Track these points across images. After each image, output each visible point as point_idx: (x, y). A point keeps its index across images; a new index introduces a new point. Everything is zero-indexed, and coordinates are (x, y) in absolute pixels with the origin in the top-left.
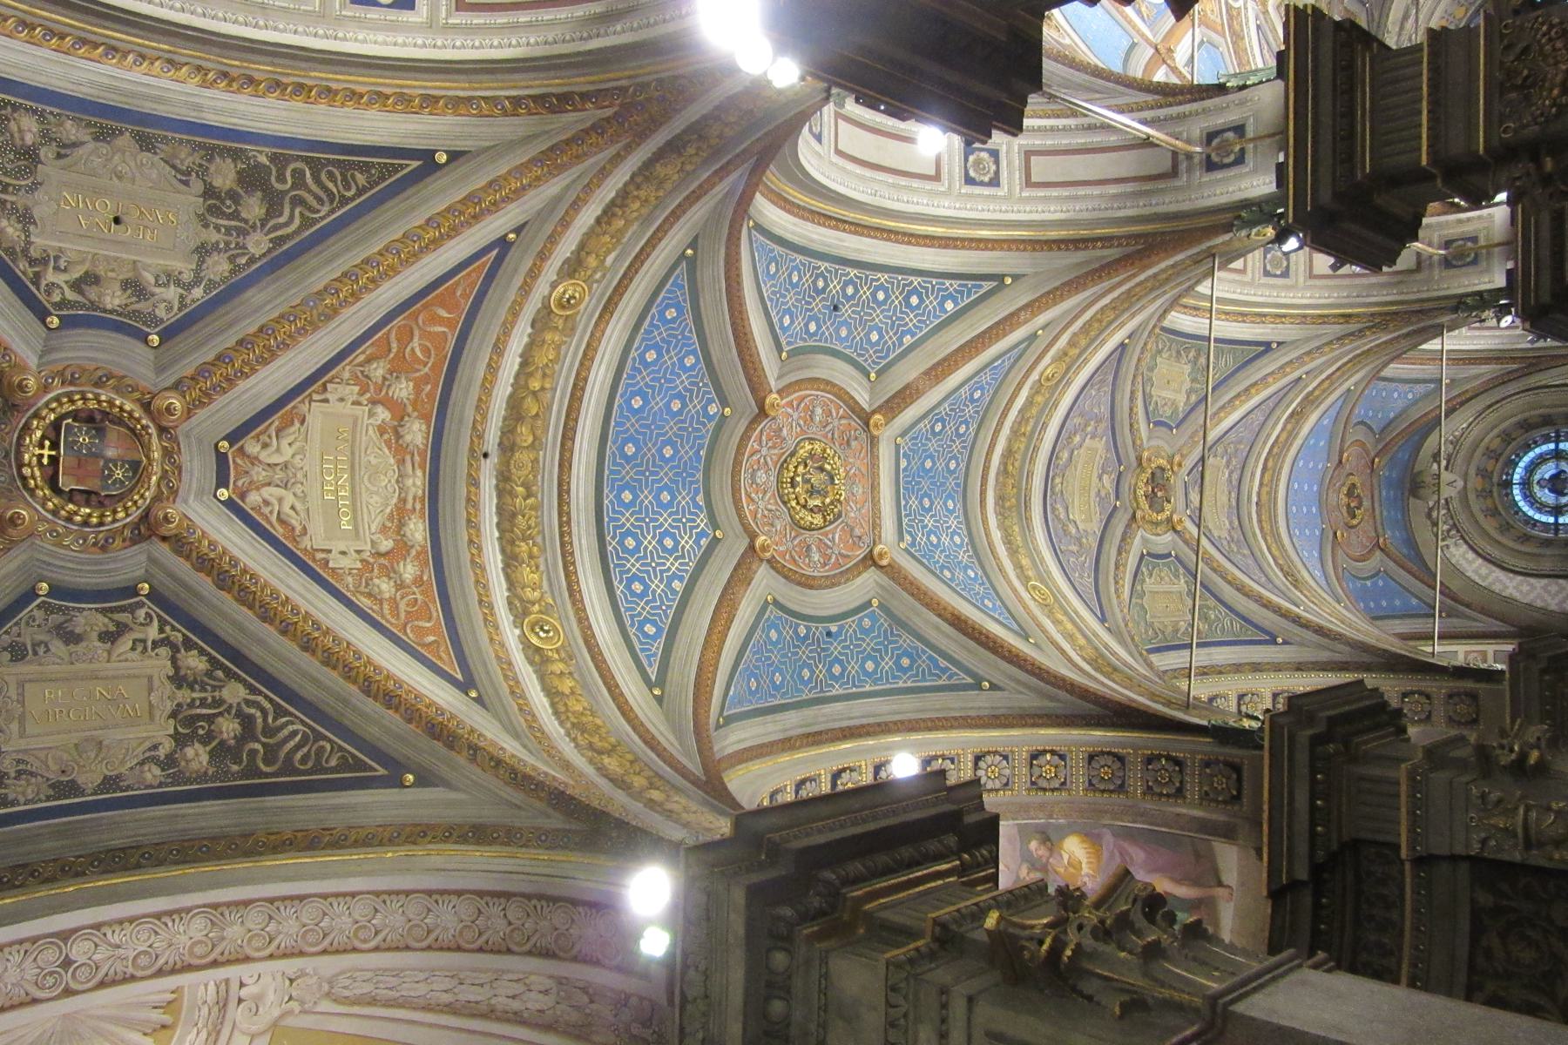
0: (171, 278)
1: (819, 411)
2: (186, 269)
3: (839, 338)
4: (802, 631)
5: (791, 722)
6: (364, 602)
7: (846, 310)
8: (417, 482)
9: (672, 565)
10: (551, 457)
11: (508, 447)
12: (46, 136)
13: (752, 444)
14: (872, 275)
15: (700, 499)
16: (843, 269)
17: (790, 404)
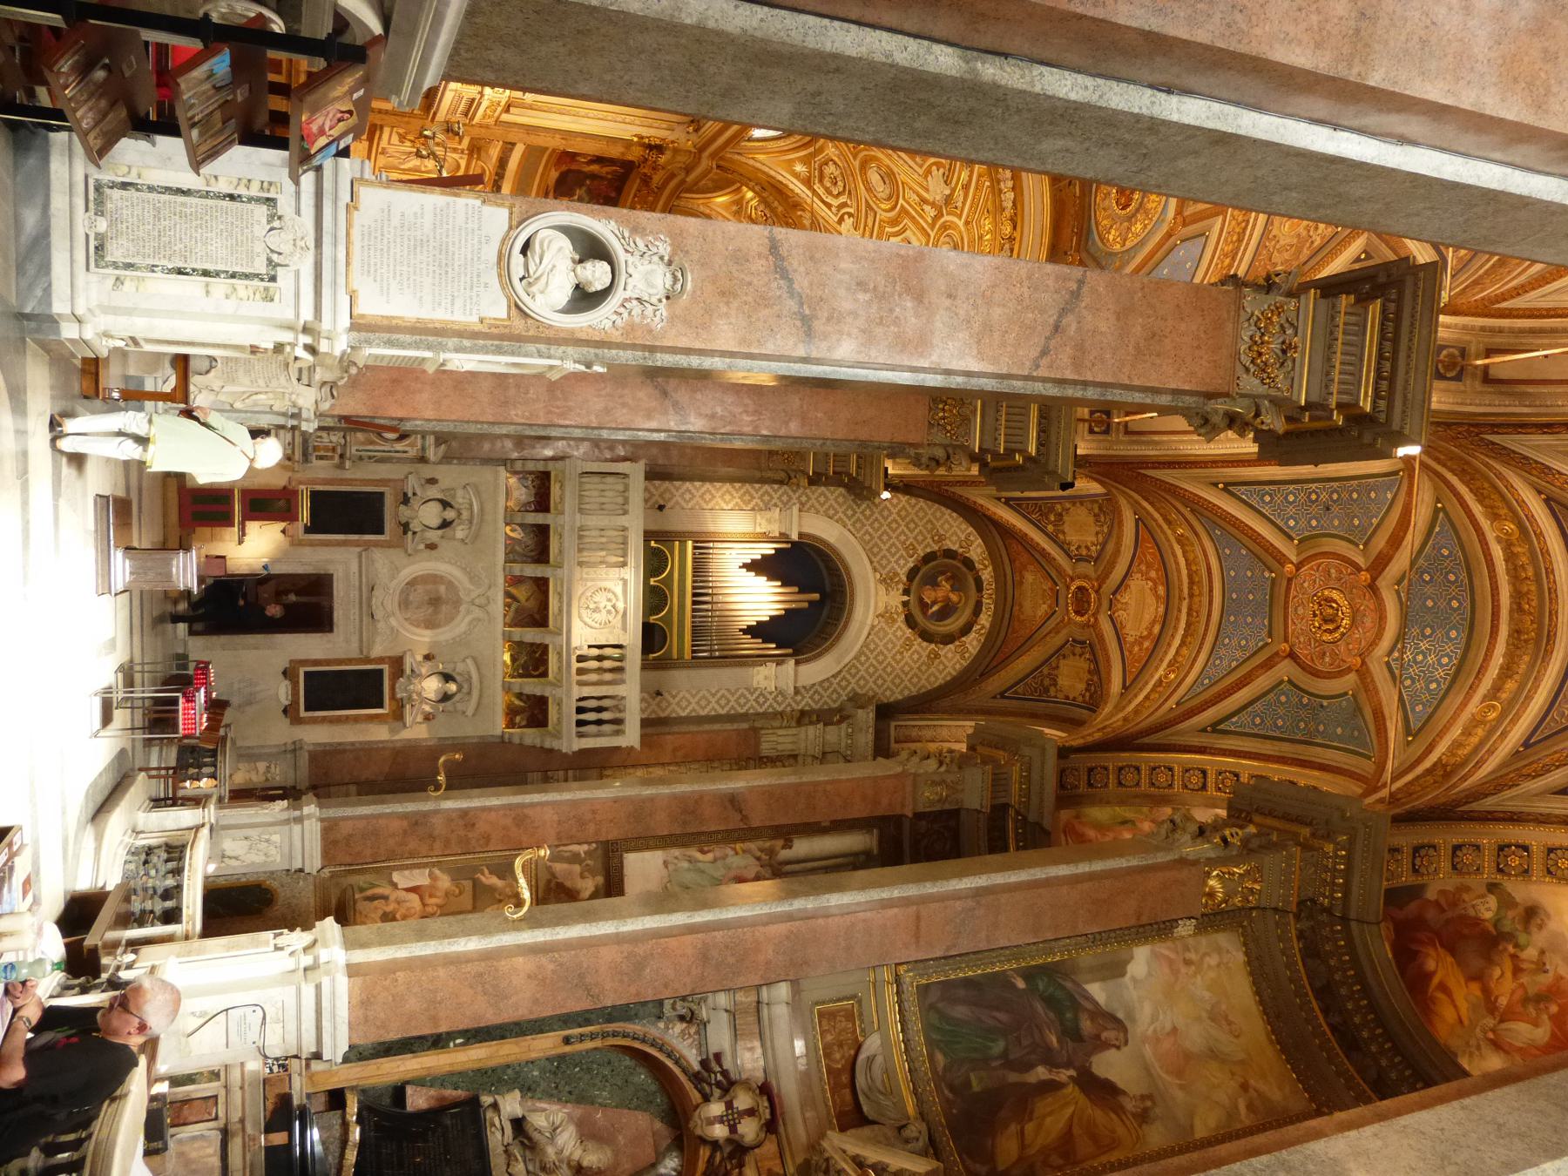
0: (1093, 544)
1: (1333, 571)
2: (1094, 539)
3: (1333, 526)
4: (1305, 701)
5: (1286, 749)
6: (1126, 653)
7: (1335, 509)
8: (1162, 609)
9: (1238, 654)
10: (1205, 600)
11: (1191, 596)
12: (1063, 509)
13: (1293, 593)
14: (1348, 484)
15: (1266, 622)
16: (1328, 485)
17: (1311, 568)
